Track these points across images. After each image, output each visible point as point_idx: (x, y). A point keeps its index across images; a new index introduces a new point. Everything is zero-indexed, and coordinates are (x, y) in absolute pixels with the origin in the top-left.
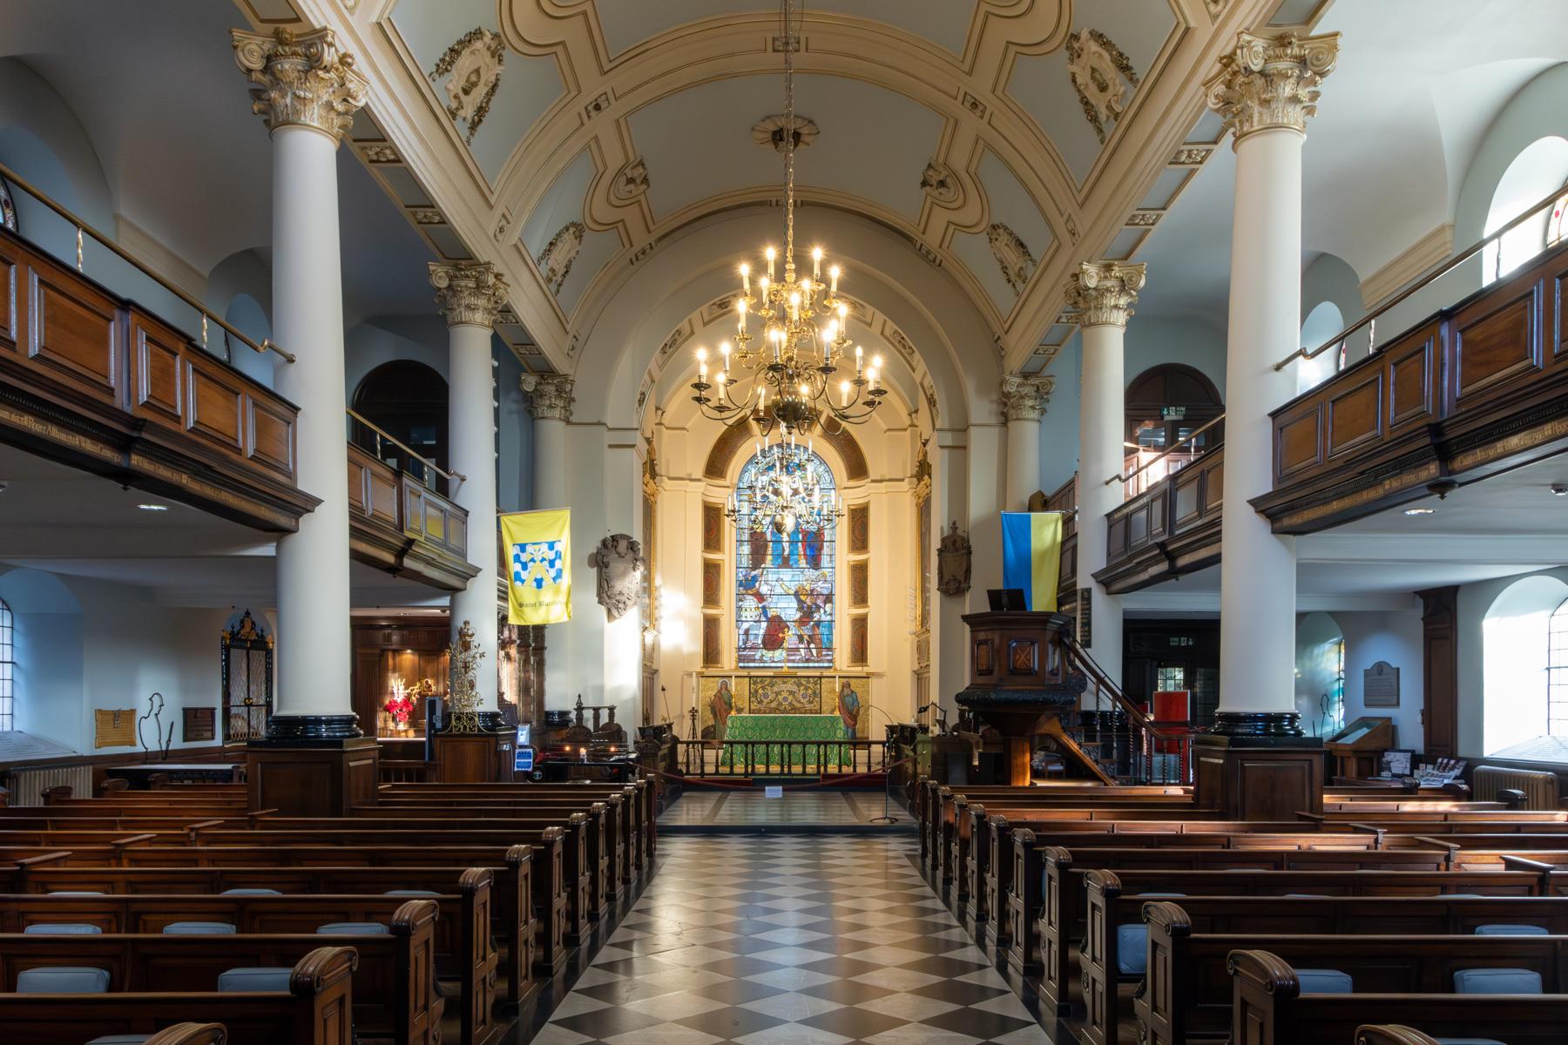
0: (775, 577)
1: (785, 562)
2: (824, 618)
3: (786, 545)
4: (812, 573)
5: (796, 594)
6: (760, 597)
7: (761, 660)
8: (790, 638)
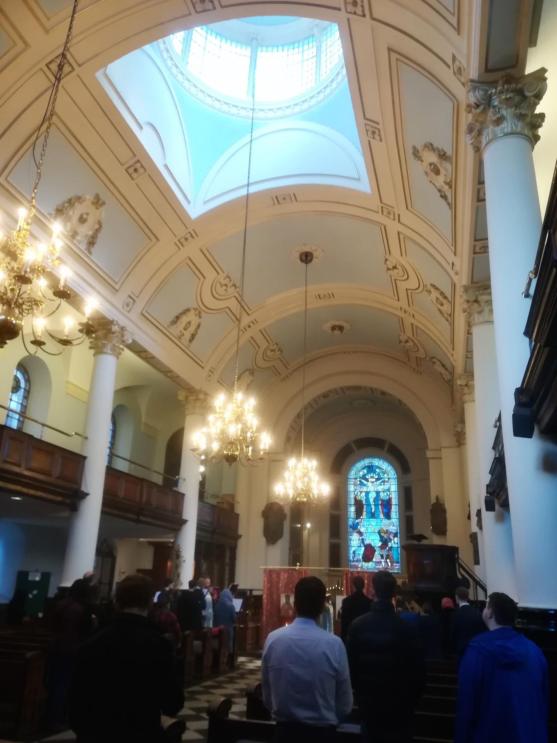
1: (373, 516)
3: (373, 507)
4: (386, 521)
5: (379, 533)
6: (361, 534)
8: (377, 557)
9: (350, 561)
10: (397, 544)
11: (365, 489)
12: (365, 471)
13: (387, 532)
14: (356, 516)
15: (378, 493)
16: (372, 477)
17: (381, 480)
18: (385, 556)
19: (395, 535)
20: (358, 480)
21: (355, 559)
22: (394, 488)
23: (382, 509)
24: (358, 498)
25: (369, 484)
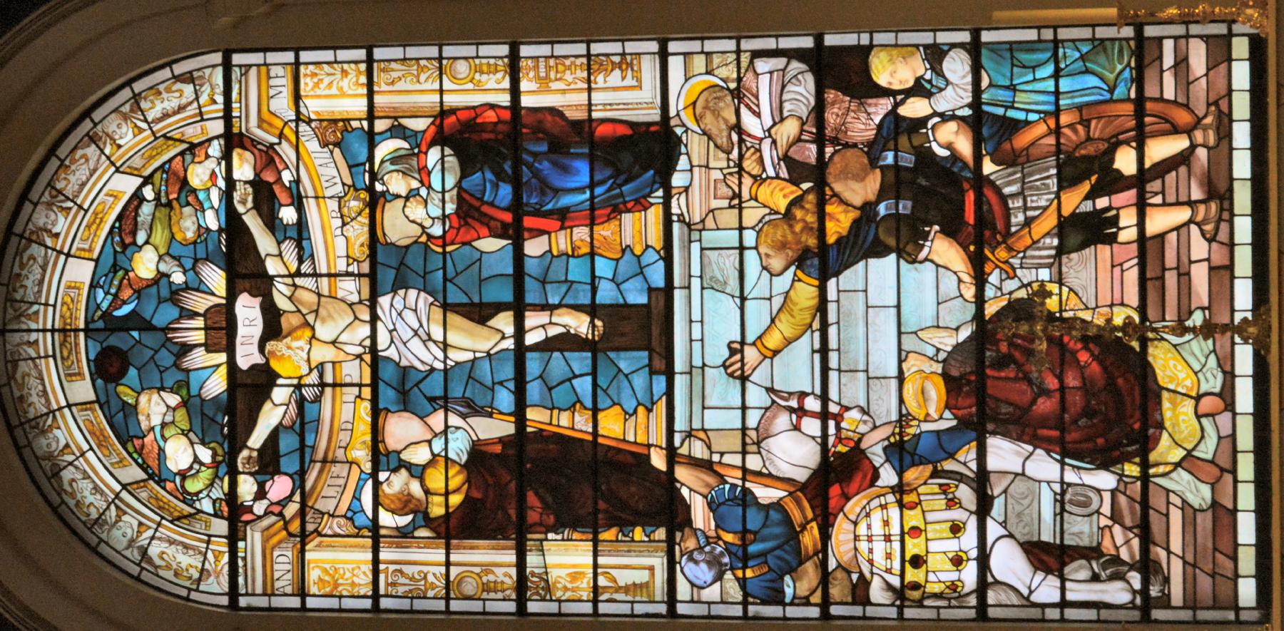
0: (722, 390)
1: (643, 329)
2: (955, 97)
3: (538, 328)
4: (697, 178)
5: (823, 261)
7: (1225, 469)
8: (1096, 288)
9: (1146, 604)
10: (935, 55)
11: (346, 414)
12: (155, 408)
13: (812, 176)
14: (648, 519)
15: (386, 268)
16: (222, 329)
17: (253, 223)
18: (1074, 201)
19: (842, 73)
20: (247, 487)
21: (1124, 544)
22: (335, 90)
23: (564, 217)
24: (446, 491)
25: (292, 358)
